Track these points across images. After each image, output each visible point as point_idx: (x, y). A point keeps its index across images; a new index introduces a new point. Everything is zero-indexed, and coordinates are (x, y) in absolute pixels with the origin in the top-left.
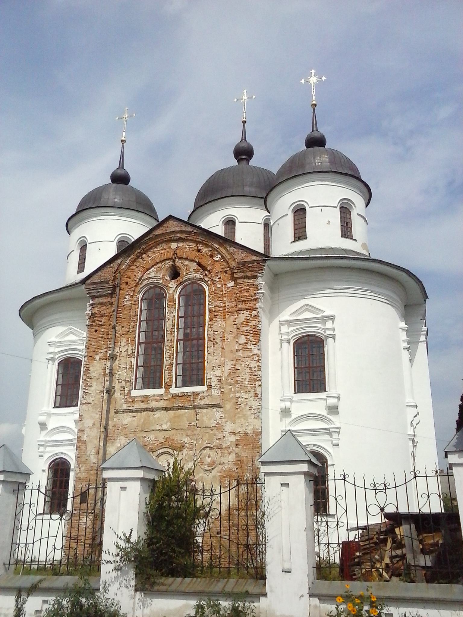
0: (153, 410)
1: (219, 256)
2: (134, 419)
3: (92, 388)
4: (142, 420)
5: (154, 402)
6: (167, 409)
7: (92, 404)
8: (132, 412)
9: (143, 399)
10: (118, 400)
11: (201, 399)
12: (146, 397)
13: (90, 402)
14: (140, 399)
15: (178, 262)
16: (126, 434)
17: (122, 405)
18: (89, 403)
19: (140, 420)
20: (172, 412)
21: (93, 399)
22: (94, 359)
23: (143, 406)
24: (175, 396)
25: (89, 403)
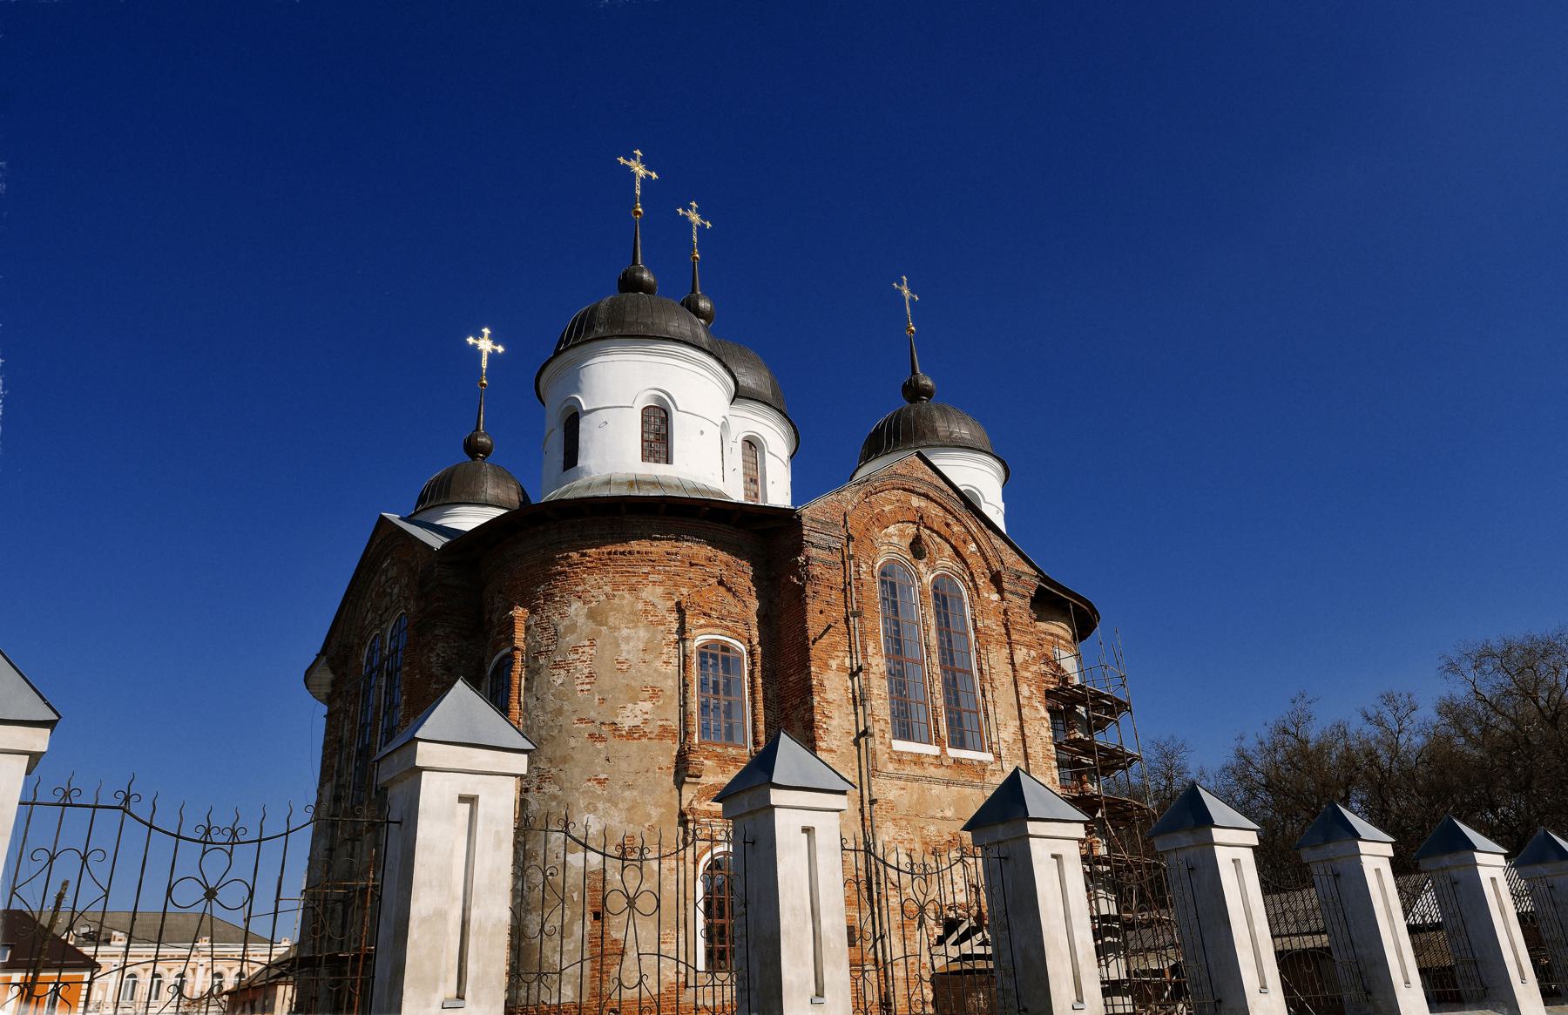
0: (930, 780)
1: (974, 545)
2: (902, 792)
3: (835, 722)
4: (915, 796)
5: (932, 768)
6: (948, 783)
7: (838, 752)
8: (900, 778)
9: (915, 759)
10: (879, 753)
11: (991, 775)
12: (919, 755)
13: (834, 747)
14: (909, 758)
15: (925, 533)
16: (895, 819)
17: (885, 765)
18: (831, 751)
19: (912, 796)
20: (954, 789)
21: (839, 743)
22: (828, 666)
23: (918, 771)
24: (958, 762)
25: (831, 751)
